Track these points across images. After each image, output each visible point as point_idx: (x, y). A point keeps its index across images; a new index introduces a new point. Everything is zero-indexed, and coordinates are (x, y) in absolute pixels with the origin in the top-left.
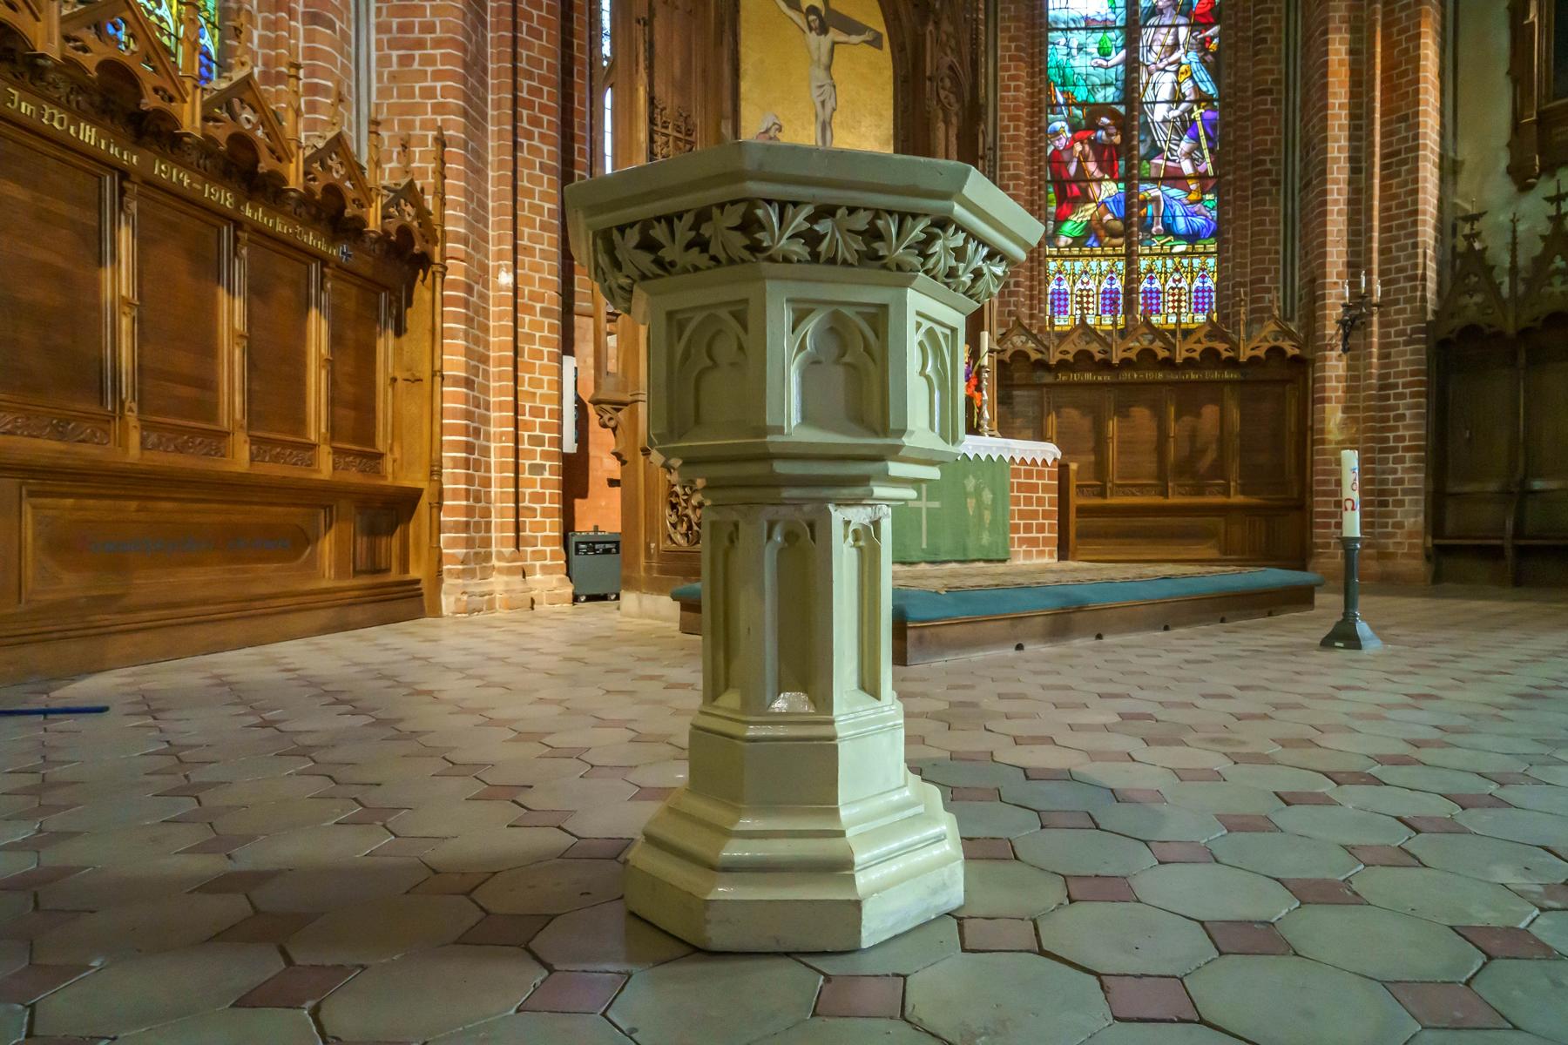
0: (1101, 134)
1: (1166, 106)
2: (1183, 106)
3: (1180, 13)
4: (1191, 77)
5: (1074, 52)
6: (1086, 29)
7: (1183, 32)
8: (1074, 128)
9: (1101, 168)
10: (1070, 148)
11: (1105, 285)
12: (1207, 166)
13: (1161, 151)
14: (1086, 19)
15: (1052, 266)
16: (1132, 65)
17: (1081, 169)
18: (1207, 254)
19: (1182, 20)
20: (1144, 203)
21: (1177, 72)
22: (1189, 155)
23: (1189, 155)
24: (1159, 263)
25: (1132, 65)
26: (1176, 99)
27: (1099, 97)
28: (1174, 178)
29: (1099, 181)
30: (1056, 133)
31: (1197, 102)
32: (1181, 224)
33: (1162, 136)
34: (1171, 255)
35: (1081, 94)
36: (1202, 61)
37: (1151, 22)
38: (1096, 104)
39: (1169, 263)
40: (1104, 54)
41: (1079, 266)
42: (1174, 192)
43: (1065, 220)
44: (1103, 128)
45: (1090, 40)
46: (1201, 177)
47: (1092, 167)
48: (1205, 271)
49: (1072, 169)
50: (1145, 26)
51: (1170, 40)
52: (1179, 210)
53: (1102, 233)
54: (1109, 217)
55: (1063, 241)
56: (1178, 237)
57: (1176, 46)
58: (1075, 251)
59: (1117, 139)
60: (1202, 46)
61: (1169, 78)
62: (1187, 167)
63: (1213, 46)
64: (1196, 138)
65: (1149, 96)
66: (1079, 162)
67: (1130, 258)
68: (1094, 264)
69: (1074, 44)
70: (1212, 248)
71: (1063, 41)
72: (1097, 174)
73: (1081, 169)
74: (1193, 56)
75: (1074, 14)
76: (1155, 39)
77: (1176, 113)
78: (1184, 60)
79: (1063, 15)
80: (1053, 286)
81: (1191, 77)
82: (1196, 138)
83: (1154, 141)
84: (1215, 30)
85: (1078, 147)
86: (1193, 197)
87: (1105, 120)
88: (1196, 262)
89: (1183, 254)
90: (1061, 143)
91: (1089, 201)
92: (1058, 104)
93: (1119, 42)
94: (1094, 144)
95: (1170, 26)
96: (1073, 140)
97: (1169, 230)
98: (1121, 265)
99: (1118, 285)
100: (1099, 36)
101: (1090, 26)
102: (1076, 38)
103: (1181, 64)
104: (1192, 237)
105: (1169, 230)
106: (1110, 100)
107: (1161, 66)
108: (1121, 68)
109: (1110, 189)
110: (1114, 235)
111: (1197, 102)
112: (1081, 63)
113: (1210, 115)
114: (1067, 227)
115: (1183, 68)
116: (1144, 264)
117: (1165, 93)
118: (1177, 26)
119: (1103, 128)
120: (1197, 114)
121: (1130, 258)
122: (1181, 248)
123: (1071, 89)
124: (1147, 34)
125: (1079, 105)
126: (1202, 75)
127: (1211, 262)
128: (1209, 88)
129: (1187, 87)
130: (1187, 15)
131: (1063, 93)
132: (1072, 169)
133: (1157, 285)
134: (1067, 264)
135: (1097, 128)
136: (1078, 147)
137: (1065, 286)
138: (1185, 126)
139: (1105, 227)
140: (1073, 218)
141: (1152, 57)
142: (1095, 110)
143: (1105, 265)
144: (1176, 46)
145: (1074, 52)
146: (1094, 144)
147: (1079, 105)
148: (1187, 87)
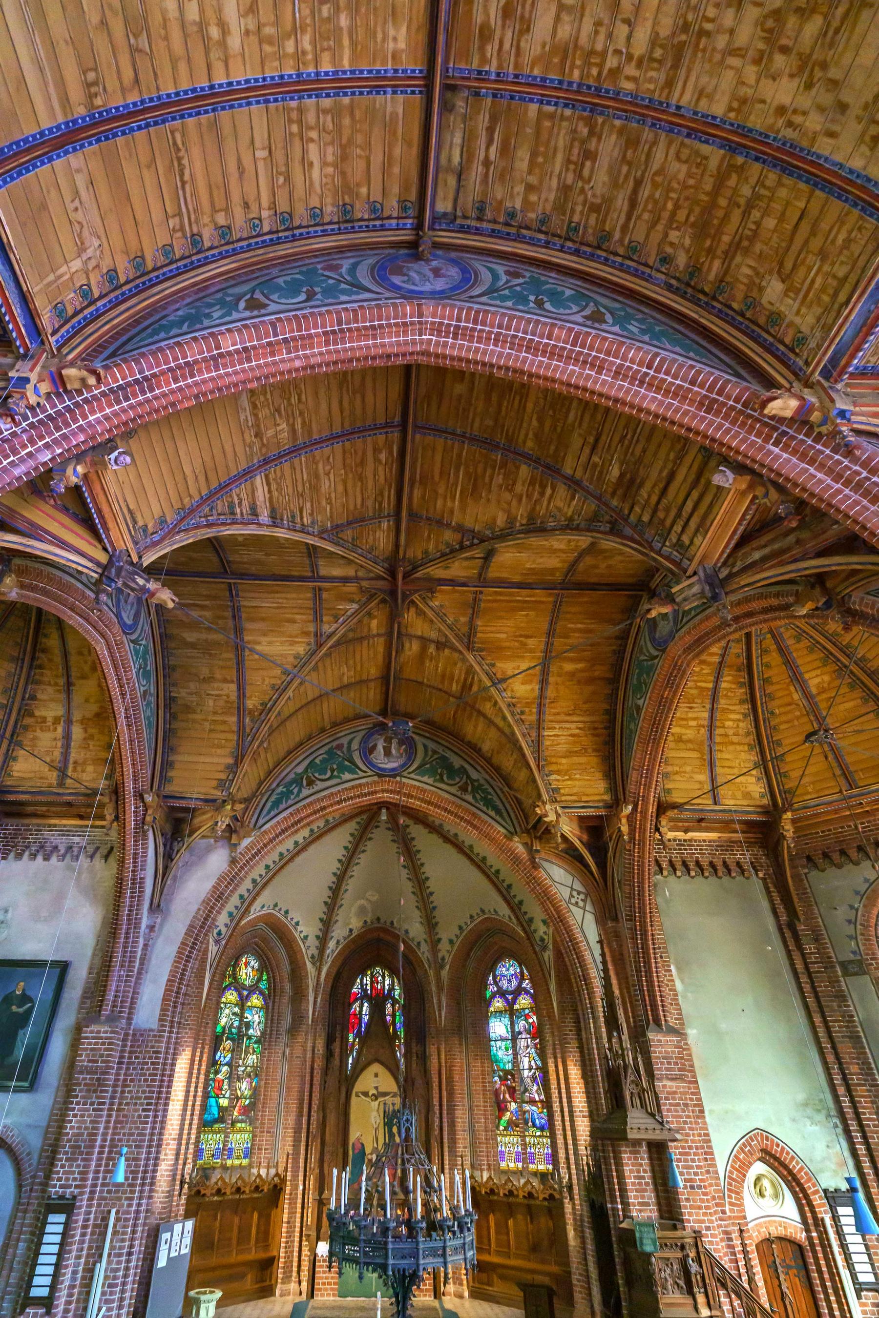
25: (515, 1054)
76: (522, 1043)
101: (502, 1039)
102: (499, 1043)
109: (513, 1106)
112: (500, 1054)
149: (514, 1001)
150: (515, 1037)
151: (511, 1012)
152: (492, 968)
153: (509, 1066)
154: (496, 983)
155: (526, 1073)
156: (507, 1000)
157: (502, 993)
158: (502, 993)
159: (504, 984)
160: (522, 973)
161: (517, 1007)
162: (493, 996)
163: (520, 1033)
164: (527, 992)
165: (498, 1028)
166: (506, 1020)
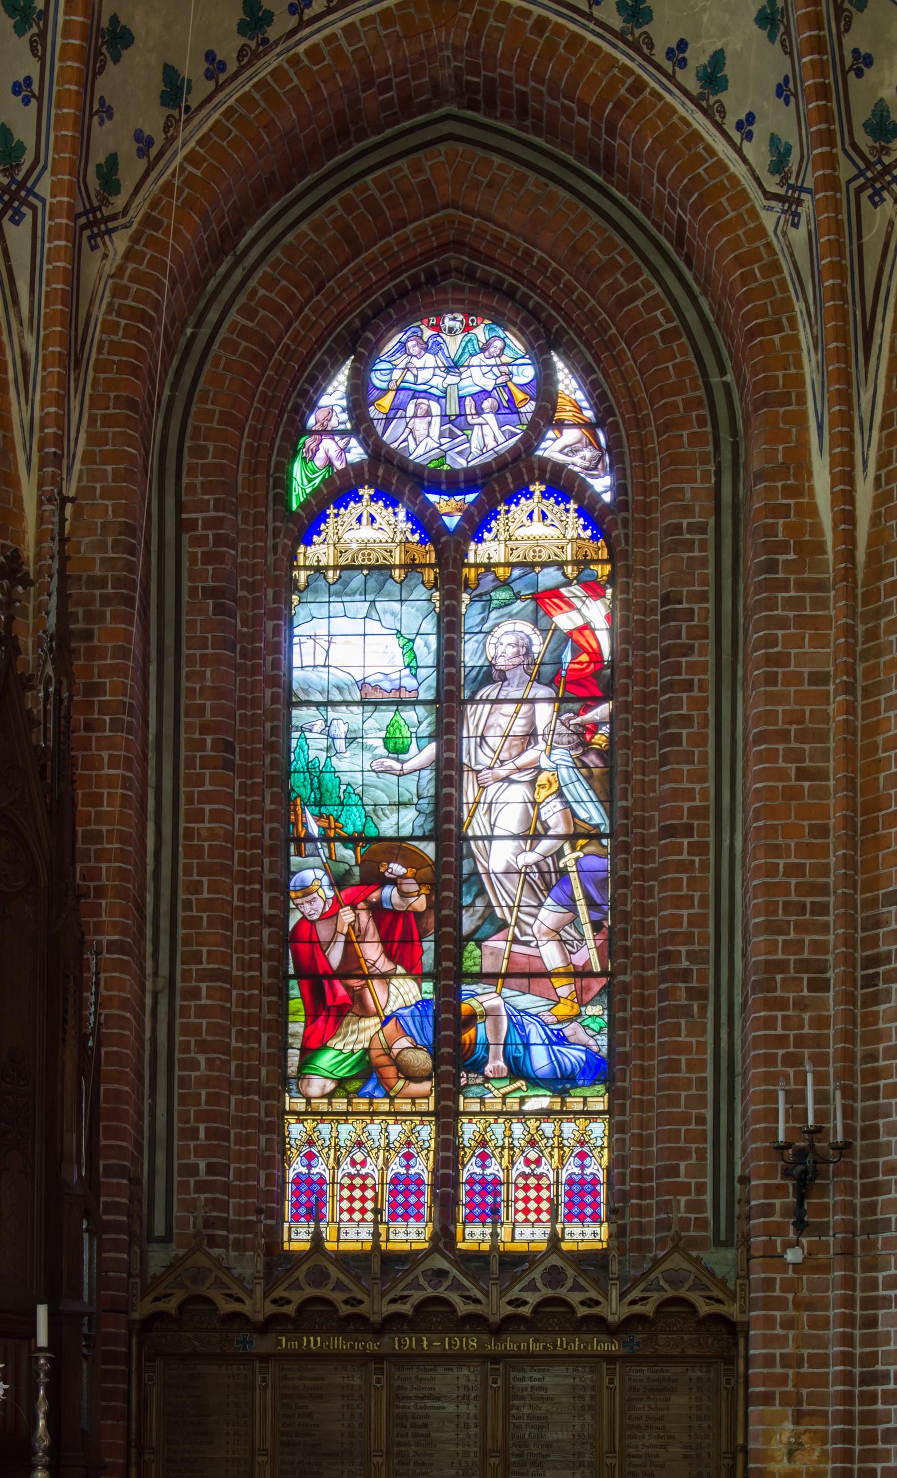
0: (389, 892)
1: (512, 845)
2: (544, 845)
3: (538, 679)
4: (560, 794)
5: (340, 744)
6: (363, 703)
7: (544, 713)
8: (338, 882)
9: (389, 954)
10: (331, 915)
11: (397, 1167)
12: (589, 954)
13: (504, 925)
14: (362, 685)
15: (296, 1130)
16: (449, 771)
17: (351, 954)
18: (590, 1115)
19: (542, 692)
20: (472, 1019)
21: (532, 783)
22: (556, 933)
23: (556, 933)
24: (499, 1129)
25: (449, 771)
26: (532, 834)
27: (387, 827)
28: (532, 976)
29: (386, 977)
30: (306, 891)
31: (571, 838)
32: (540, 1059)
33: (504, 896)
34: (521, 1115)
35: (353, 821)
36: (580, 764)
37: (484, 693)
38: (379, 839)
39: (518, 1129)
40: (396, 749)
41: (346, 1131)
42: (525, 1001)
43: (323, 1047)
44: (394, 882)
45: (370, 724)
46: (580, 974)
47: (372, 952)
48: (584, 1140)
49: (335, 956)
50: (472, 700)
51: (519, 727)
52: (535, 1034)
53: (391, 1072)
54: (405, 1042)
55: (317, 1086)
56: (535, 1081)
57: (530, 736)
58: (340, 1104)
59: (420, 903)
60: (582, 737)
61: (518, 793)
62: (552, 956)
63: (600, 739)
64: (570, 905)
65: (477, 827)
66: (348, 943)
67: (447, 1118)
68: (374, 1129)
69: (340, 730)
70: (599, 1104)
71: (319, 725)
72: (384, 965)
73: (351, 954)
74: (561, 755)
75: (338, 676)
76: (490, 724)
77: (531, 858)
78: (545, 763)
79: (319, 677)
80: (297, 1168)
81: (560, 794)
82: (570, 905)
83: (489, 906)
84: (602, 711)
85: (347, 915)
86: (563, 1010)
87: (397, 869)
88: (568, 1129)
89: (545, 1114)
90: (314, 908)
91: (365, 1013)
92: (309, 838)
93: (425, 729)
94: (378, 911)
95: (521, 701)
96: (337, 905)
97: (517, 1069)
98: (427, 1132)
99: (422, 1167)
100: (386, 716)
102: (346, 719)
103: (539, 770)
104: (560, 1082)
105: (517, 1069)
106: (406, 832)
107: (502, 772)
108: (428, 775)
109: (404, 993)
110: (412, 1078)
111: (571, 838)
112: (350, 765)
113: (594, 863)
114: (326, 1060)
115: (543, 778)
116: (469, 1130)
117: (510, 820)
118: (533, 701)
119: (394, 882)
120: (569, 860)
121: (447, 1118)
122: (540, 1101)
123: (333, 810)
124: (476, 717)
125: (351, 840)
126: (579, 790)
127: (598, 1129)
128: (592, 813)
129: (553, 814)
130: (553, 682)
131: (319, 817)
132: (335, 956)
133: (494, 1169)
134: (325, 1128)
135: (384, 881)
136: (347, 915)
137: (320, 1168)
138: (549, 881)
139: (397, 1063)
140: (336, 1043)
141: (485, 758)
142: (378, 849)
143: (395, 1130)
144: (530, 736)
145: (340, 744)
146: (378, 911)
147: (351, 840)
148: (553, 814)
149: (478, 525)
150: (451, 696)
151: (446, 570)
152: (359, 342)
153: (405, 822)
154: (361, 424)
155: (500, 857)
156: (425, 524)
157: (391, 477)
158: (391, 477)
159: (420, 439)
160: (544, 390)
161: (487, 550)
162: (340, 490)
163: (490, 674)
164: (562, 486)
165: (350, 647)
166: (417, 614)
